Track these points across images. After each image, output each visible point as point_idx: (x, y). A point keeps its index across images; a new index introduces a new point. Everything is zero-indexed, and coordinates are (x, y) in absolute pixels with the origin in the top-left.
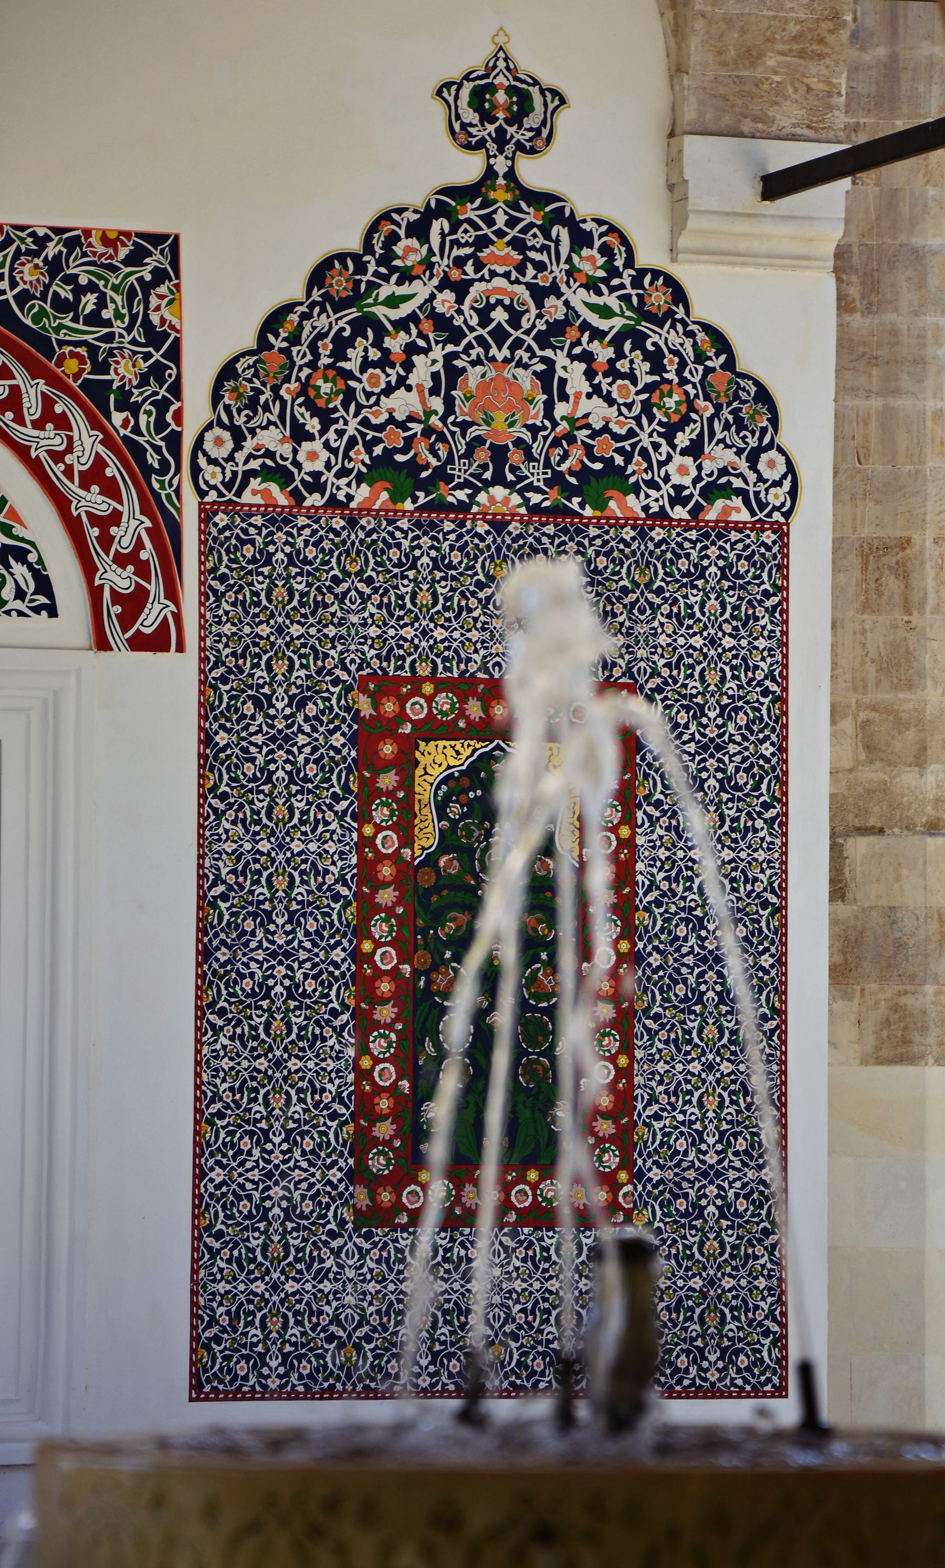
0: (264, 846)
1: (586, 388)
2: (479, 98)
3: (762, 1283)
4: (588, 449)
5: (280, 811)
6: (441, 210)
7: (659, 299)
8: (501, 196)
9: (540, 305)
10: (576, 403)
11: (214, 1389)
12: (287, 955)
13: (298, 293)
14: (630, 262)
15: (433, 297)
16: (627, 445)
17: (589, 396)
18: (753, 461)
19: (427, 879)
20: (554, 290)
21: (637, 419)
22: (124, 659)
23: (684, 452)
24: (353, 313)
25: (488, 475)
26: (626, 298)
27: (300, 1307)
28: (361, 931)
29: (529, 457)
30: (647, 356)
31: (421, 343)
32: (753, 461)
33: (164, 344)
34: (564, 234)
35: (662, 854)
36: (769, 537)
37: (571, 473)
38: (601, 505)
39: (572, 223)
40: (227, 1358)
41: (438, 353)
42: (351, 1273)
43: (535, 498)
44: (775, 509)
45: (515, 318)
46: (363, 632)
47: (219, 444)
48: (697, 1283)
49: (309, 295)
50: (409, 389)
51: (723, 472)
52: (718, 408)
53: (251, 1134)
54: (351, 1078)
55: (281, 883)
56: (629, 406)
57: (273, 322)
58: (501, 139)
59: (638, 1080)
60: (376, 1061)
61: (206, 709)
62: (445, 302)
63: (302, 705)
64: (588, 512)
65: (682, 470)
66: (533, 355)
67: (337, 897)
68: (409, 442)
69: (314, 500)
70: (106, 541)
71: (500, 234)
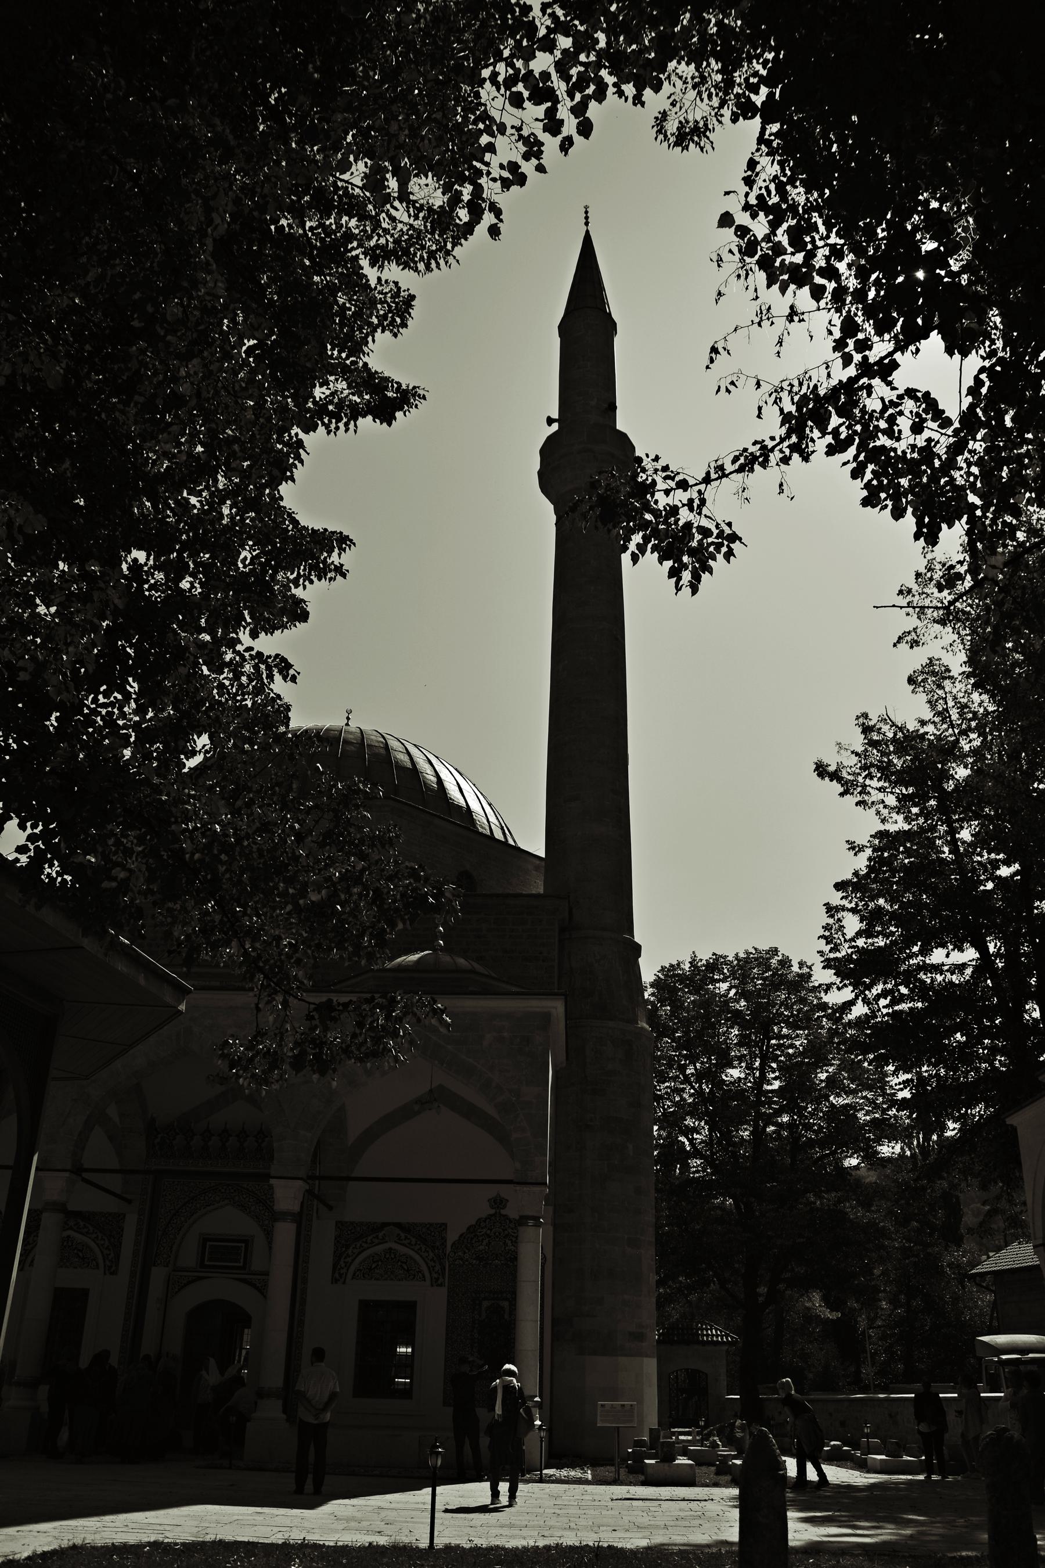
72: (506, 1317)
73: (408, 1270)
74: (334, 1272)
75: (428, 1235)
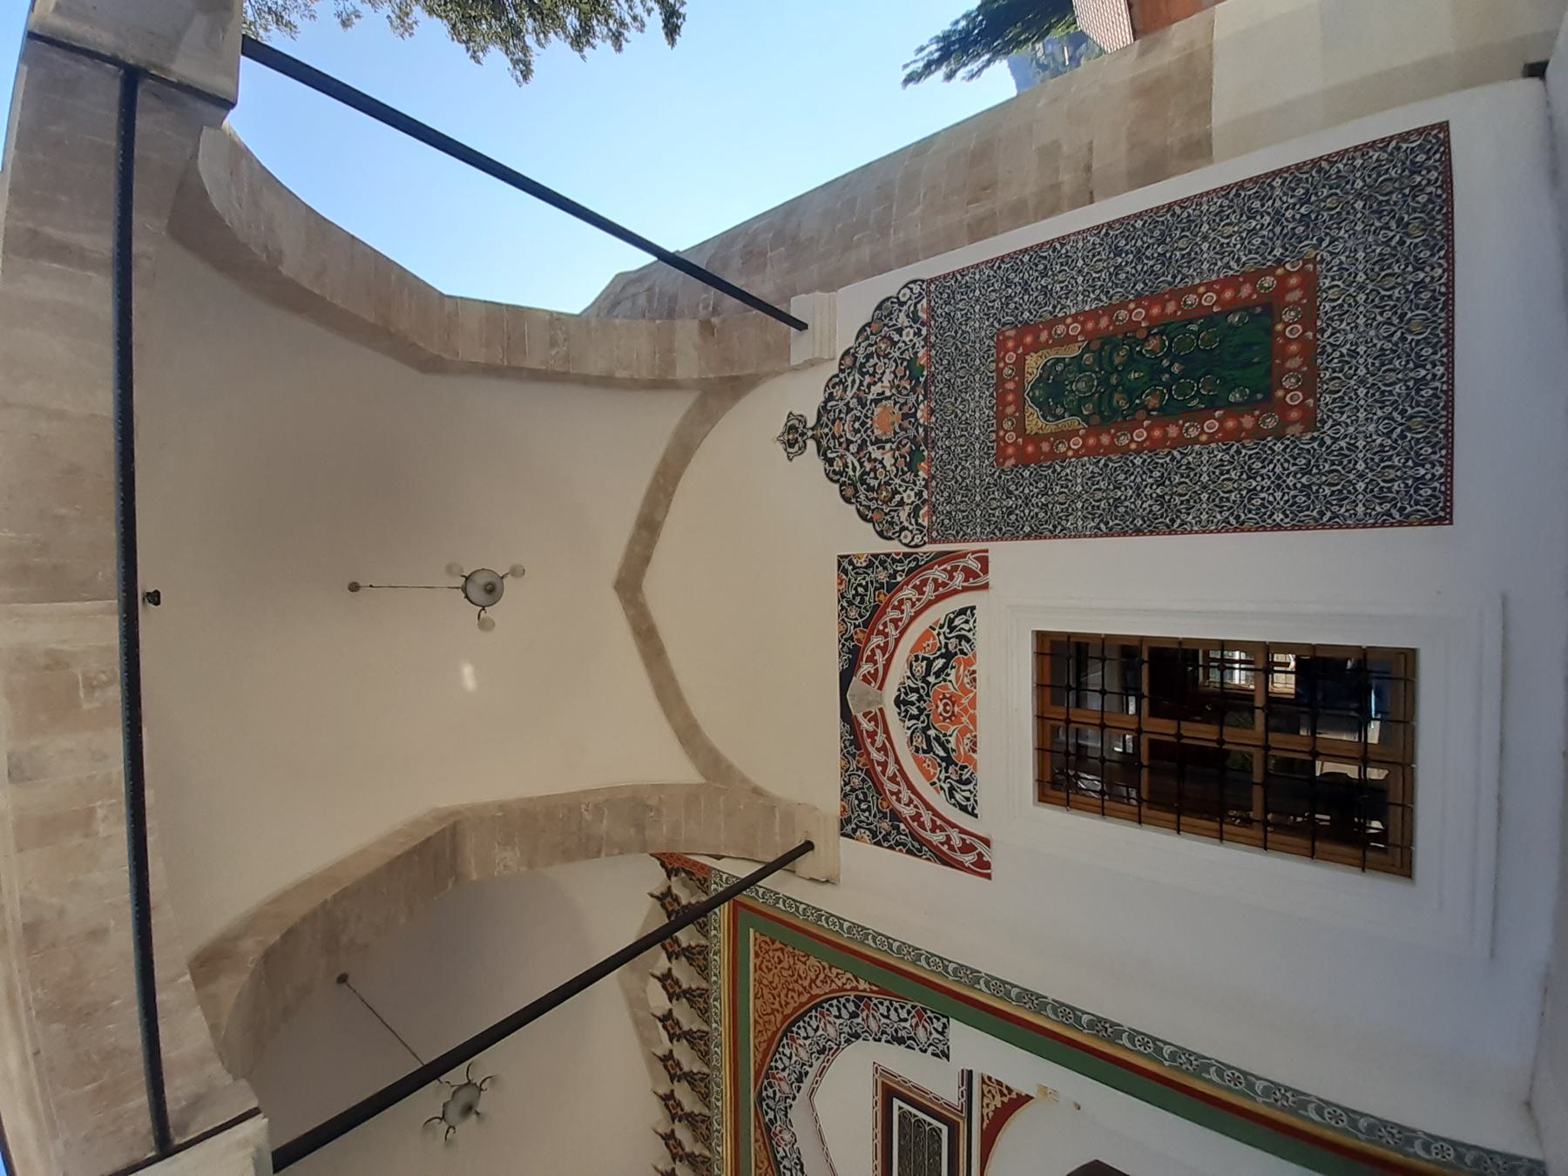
0: (1079, 505)
2: (791, 445)
3: (1359, 162)
5: (1061, 498)
7: (848, 361)
8: (819, 432)
11: (1443, 509)
12: (1138, 488)
13: (853, 508)
18: (902, 304)
19: (1096, 419)
20: (847, 404)
22: (992, 577)
27: (1377, 459)
28: (1125, 451)
32: (902, 304)
33: (875, 561)
35: (1080, 297)
36: (933, 287)
39: (826, 402)
40: (1417, 503)
42: (1351, 429)
45: (858, 418)
46: (978, 467)
47: (906, 537)
48: (1359, 205)
53: (1250, 499)
54: (1213, 445)
55: (1099, 495)
57: (864, 517)
58: (803, 434)
59: (1214, 278)
60: (1203, 431)
61: (1014, 537)
62: (853, 448)
63: (1011, 493)
67: (1106, 465)
68: (903, 456)
69: (925, 496)
70: (944, 585)
72: (1073, 351)
73: (948, 656)
74: (959, 866)
75: (867, 599)
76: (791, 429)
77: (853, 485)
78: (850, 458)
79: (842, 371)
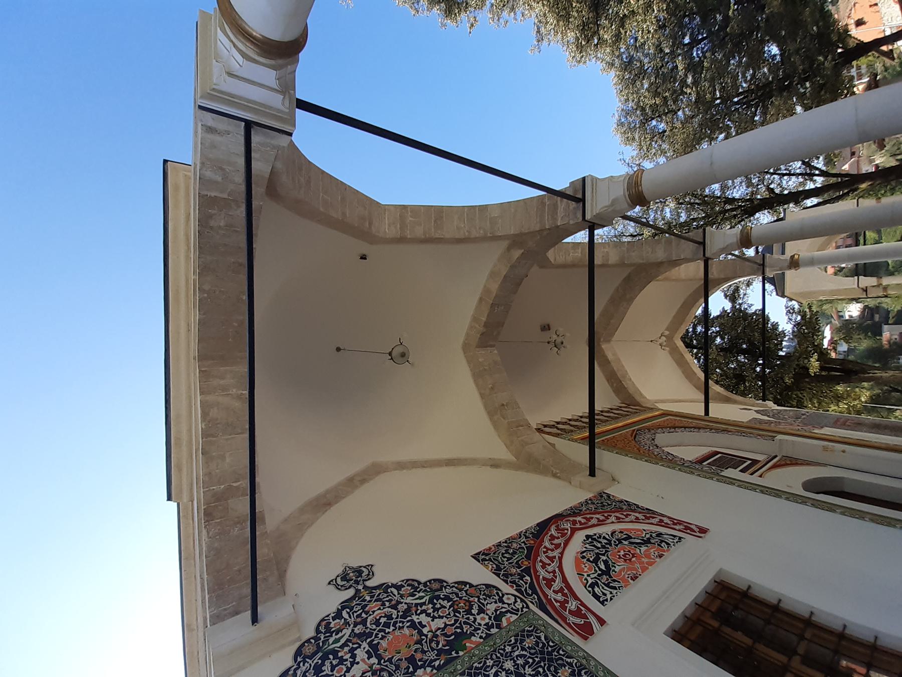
1: (430, 619)
2: (343, 579)
4: (445, 635)
6: (343, 608)
7: (435, 586)
9: (396, 609)
10: (430, 626)
14: (419, 583)
15: (353, 630)
16: (457, 625)
17: (433, 620)
20: (399, 603)
21: (455, 616)
23: (478, 614)
24: (320, 654)
25: (411, 669)
26: (425, 591)
29: (424, 652)
30: (443, 600)
31: (355, 646)
34: (393, 590)
37: (443, 646)
38: (464, 648)
39: (393, 586)
41: (365, 645)
43: (437, 663)
44: (522, 609)
45: (389, 617)
49: (295, 660)
50: (358, 663)
51: (496, 610)
52: (478, 597)
56: (449, 614)
64: (461, 653)
65: (483, 619)
66: (403, 622)
71: (370, 601)
76: (358, 571)
77: (319, 649)
78: (347, 632)
79: (425, 584)
